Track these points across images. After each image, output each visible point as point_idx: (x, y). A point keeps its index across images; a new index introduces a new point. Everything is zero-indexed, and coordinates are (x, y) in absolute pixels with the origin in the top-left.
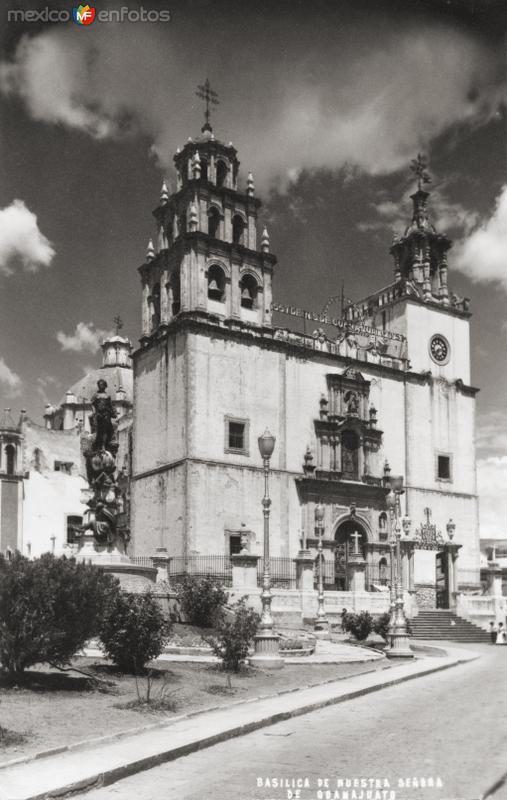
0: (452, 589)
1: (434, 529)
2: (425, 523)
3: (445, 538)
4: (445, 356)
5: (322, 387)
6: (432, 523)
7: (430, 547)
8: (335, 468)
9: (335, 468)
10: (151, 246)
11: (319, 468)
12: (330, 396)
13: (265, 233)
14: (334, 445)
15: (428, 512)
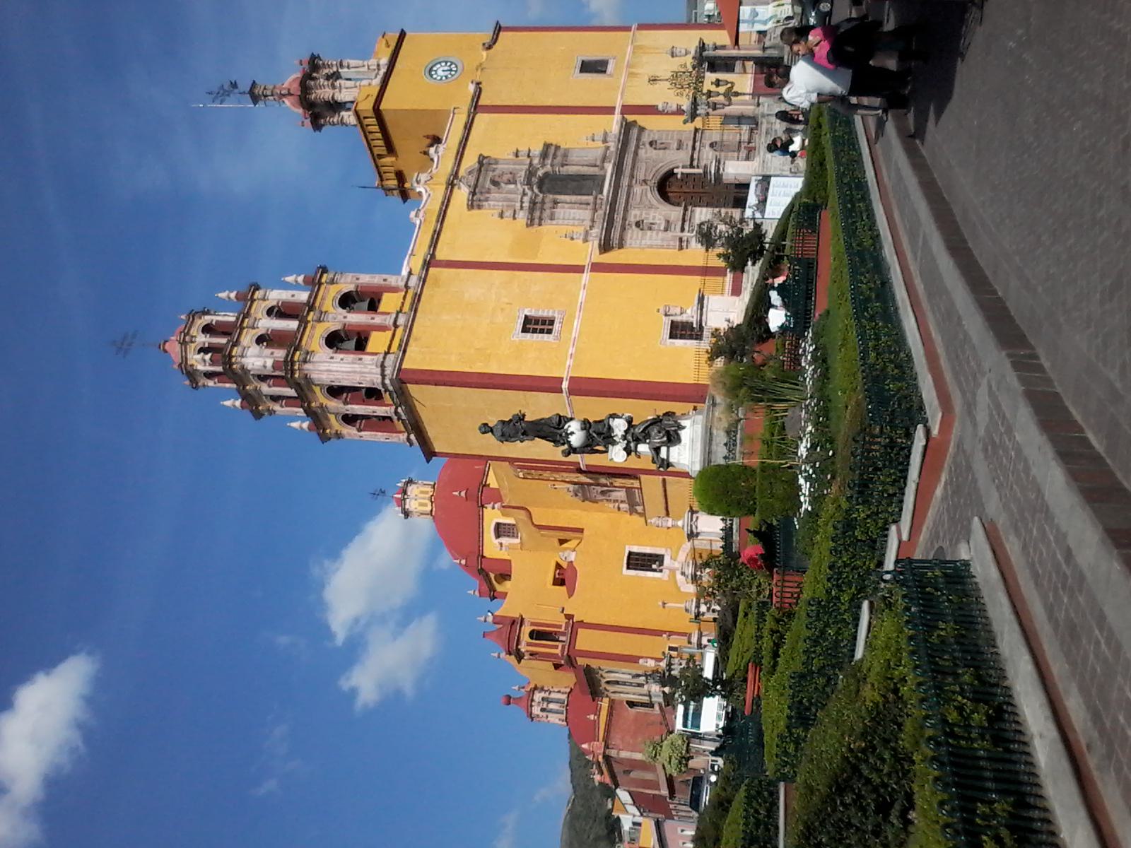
0: (758, 53)
1: (677, 73)
2: (668, 84)
3: (689, 60)
4: (452, 63)
5: (488, 215)
6: (669, 75)
7: (700, 80)
8: (588, 204)
9: (588, 204)
10: (295, 425)
11: (588, 223)
12: (494, 207)
13: (290, 279)
14: (556, 203)
15: (653, 80)
